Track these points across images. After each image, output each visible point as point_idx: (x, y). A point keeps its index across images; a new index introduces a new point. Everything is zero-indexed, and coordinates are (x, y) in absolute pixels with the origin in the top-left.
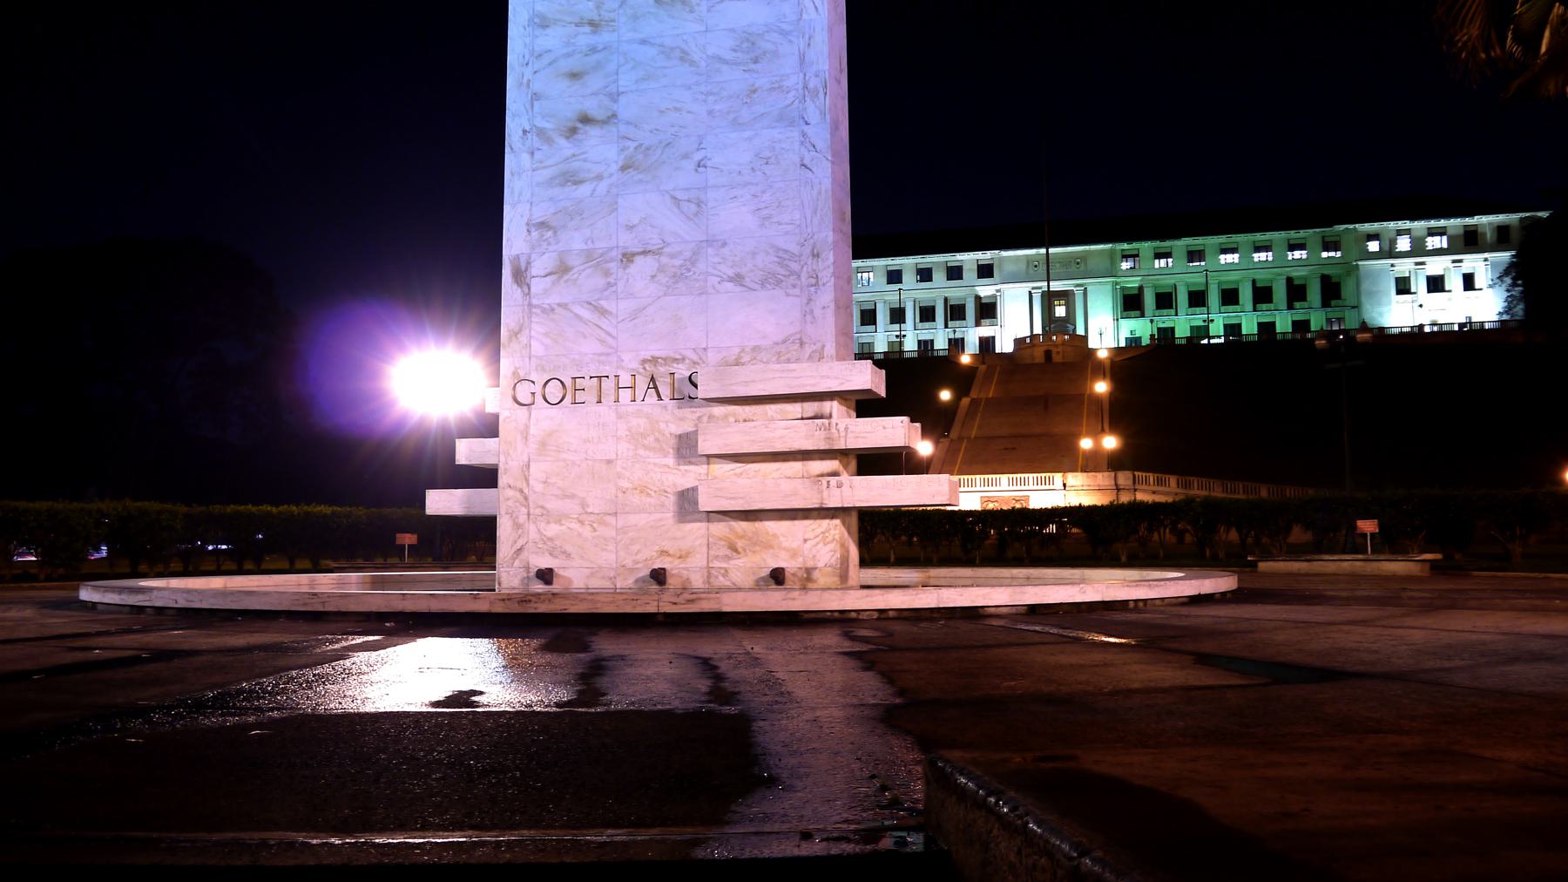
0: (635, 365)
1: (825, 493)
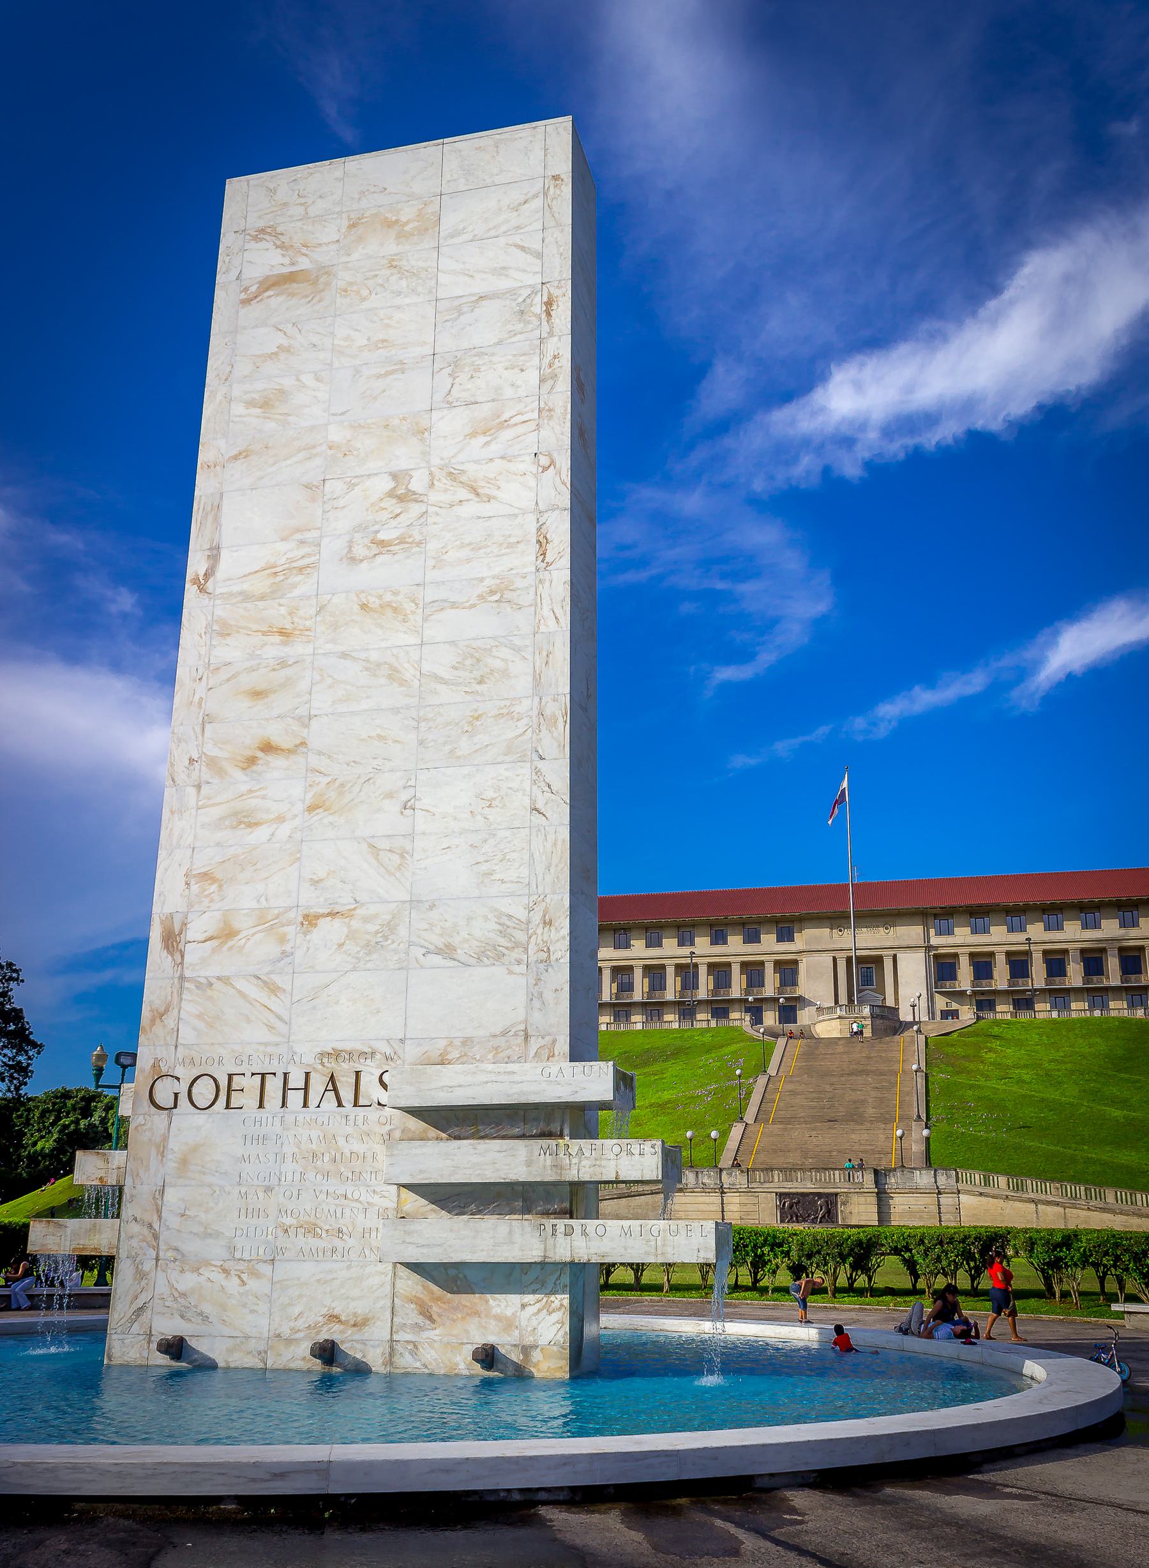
0: (309, 1059)
1: (550, 1241)
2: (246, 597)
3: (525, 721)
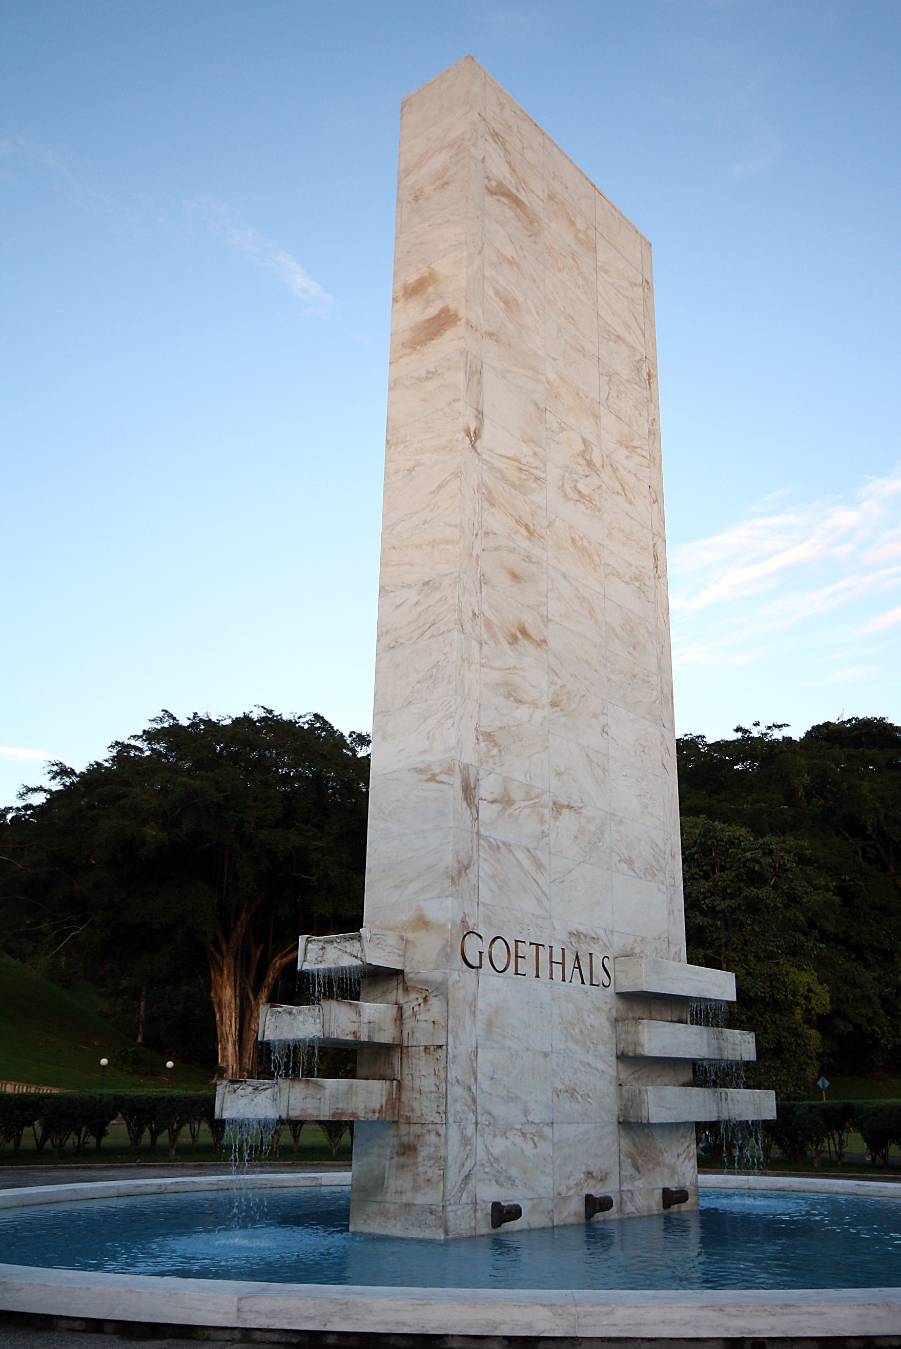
0: (564, 937)
2: (504, 479)
3: (655, 692)
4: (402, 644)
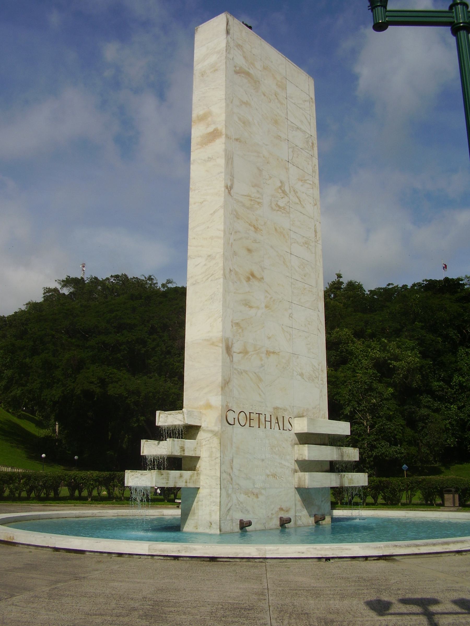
0: (272, 410)
4: (198, 283)
